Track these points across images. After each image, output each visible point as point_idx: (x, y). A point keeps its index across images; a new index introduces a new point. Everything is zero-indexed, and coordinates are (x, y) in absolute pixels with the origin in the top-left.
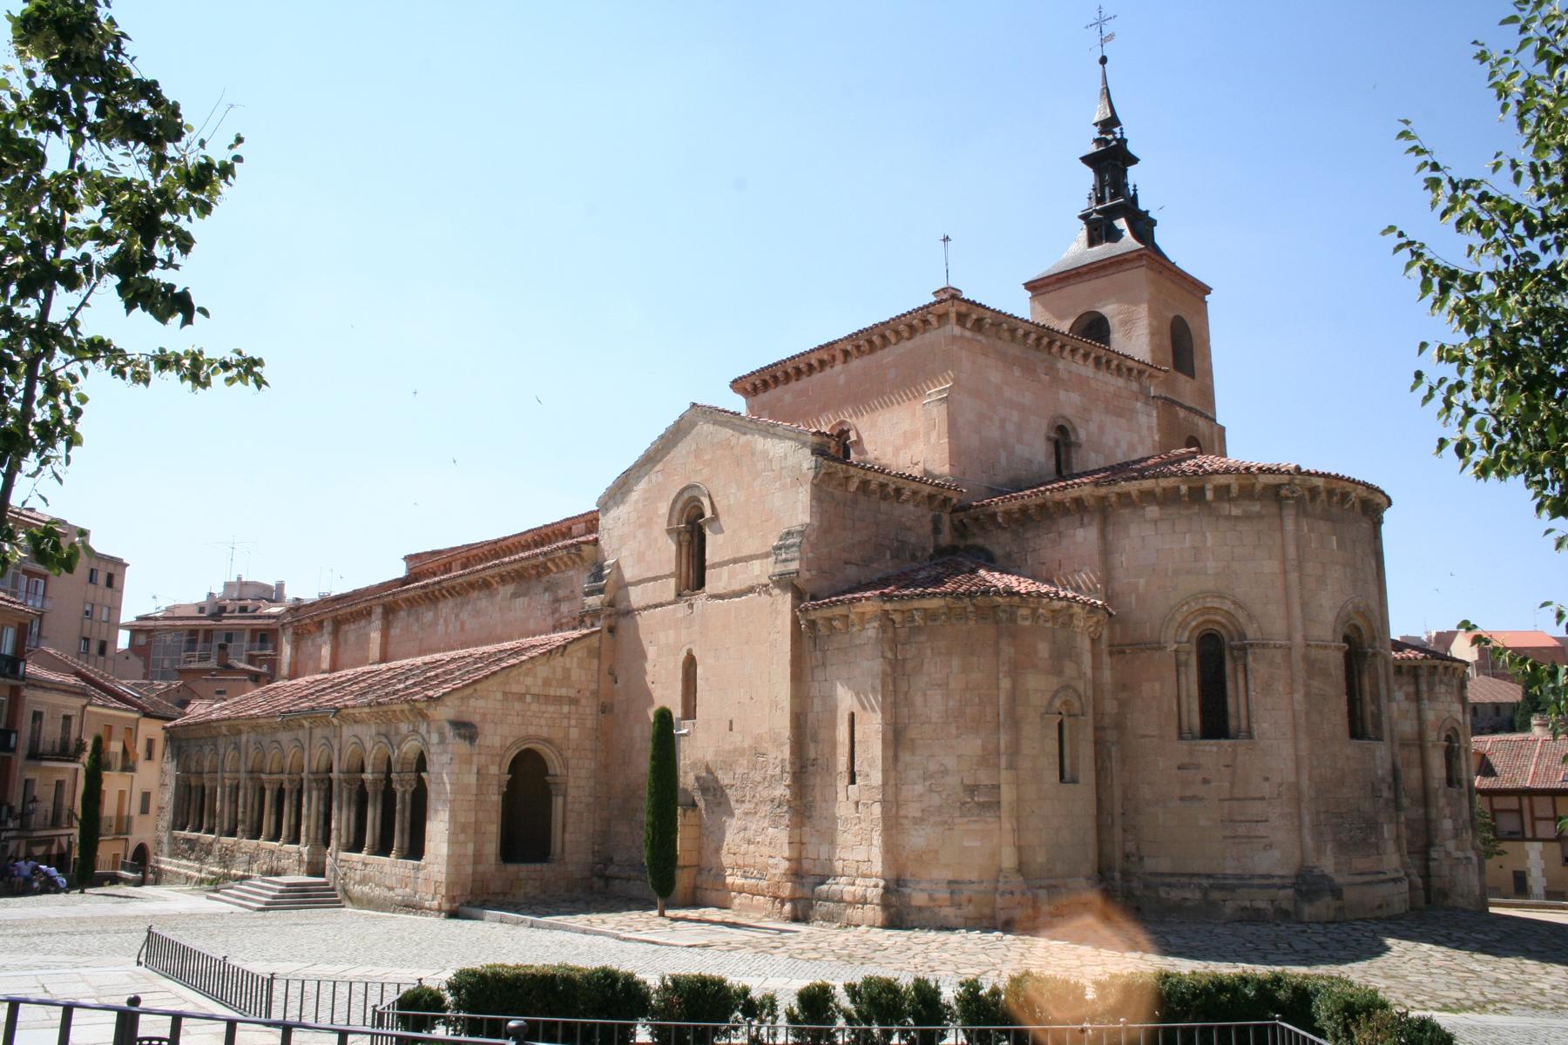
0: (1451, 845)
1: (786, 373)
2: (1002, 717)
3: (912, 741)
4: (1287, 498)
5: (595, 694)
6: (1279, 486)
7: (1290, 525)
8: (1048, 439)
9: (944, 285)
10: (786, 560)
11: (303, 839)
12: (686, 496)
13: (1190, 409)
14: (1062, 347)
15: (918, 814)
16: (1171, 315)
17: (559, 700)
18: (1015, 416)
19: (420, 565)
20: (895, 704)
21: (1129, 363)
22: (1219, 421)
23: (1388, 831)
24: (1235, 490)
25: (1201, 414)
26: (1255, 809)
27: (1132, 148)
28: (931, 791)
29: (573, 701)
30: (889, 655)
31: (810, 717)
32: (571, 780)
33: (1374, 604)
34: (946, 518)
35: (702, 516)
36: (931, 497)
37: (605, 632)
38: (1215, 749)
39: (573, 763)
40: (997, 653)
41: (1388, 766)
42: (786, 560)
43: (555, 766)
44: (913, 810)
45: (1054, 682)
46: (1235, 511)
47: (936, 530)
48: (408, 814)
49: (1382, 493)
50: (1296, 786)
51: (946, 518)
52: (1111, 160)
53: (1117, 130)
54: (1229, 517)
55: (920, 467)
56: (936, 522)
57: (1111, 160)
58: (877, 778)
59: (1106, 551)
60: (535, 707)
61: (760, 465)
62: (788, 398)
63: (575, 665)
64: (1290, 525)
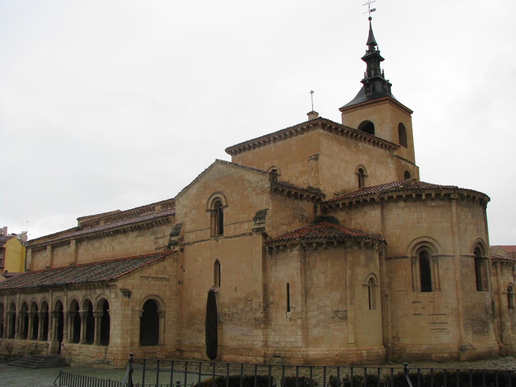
0: (510, 332)
1: (249, 146)
2: (348, 284)
3: (312, 294)
4: (453, 199)
5: (176, 277)
6: (450, 194)
7: (454, 209)
8: (356, 173)
9: (311, 111)
10: (259, 223)
11: (49, 338)
12: (214, 196)
13: (405, 160)
14: (361, 138)
15: (315, 323)
16: (398, 123)
17: (162, 279)
19: (85, 222)
20: (305, 280)
21: (386, 143)
23: (491, 326)
24: (433, 195)
25: (410, 162)
26: (442, 318)
27: (382, 54)
28: (320, 313)
29: (167, 280)
30: (303, 261)
31: (270, 286)
32: (167, 313)
33: (484, 239)
34: (319, 206)
35: (221, 205)
36: (313, 198)
37: (179, 251)
38: (427, 296)
39: (167, 305)
40: (346, 260)
41: (490, 301)
42: (259, 223)
43: (161, 308)
44: (313, 321)
46: (433, 204)
47: (315, 211)
48: (100, 327)
49: (487, 196)
50: (457, 309)
51: (319, 206)
52: (373, 58)
53: (376, 47)
54: (431, 206)
55: (307, 185)
56: (315, 208)
57: (373, 58)
58: (299, 309)
59: (383, 219)
60: (153, 282)
61: (247, 186)
62: (250, 156)
63: (168, 265)
64: (454, 209)
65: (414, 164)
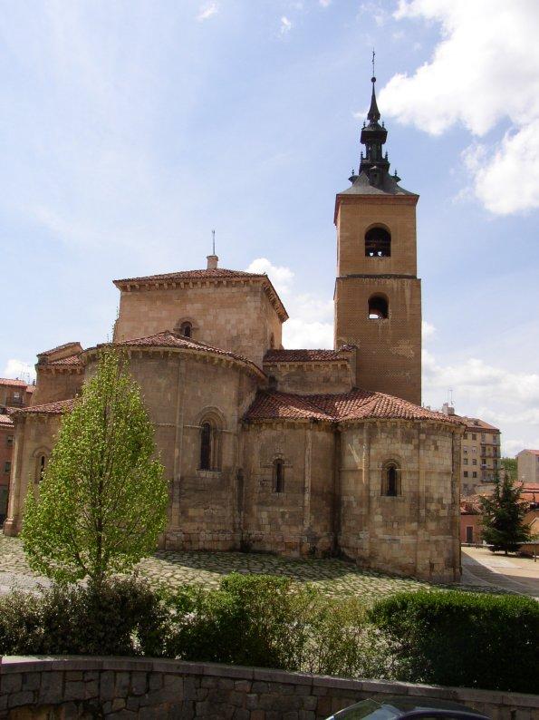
0: (380, 532)
9: (212, 254)
18: (155, 324)
22: (418, 277)
45: (36, 445)
52: (374, 136)
57: (374, 136)
65: (414, 277)
